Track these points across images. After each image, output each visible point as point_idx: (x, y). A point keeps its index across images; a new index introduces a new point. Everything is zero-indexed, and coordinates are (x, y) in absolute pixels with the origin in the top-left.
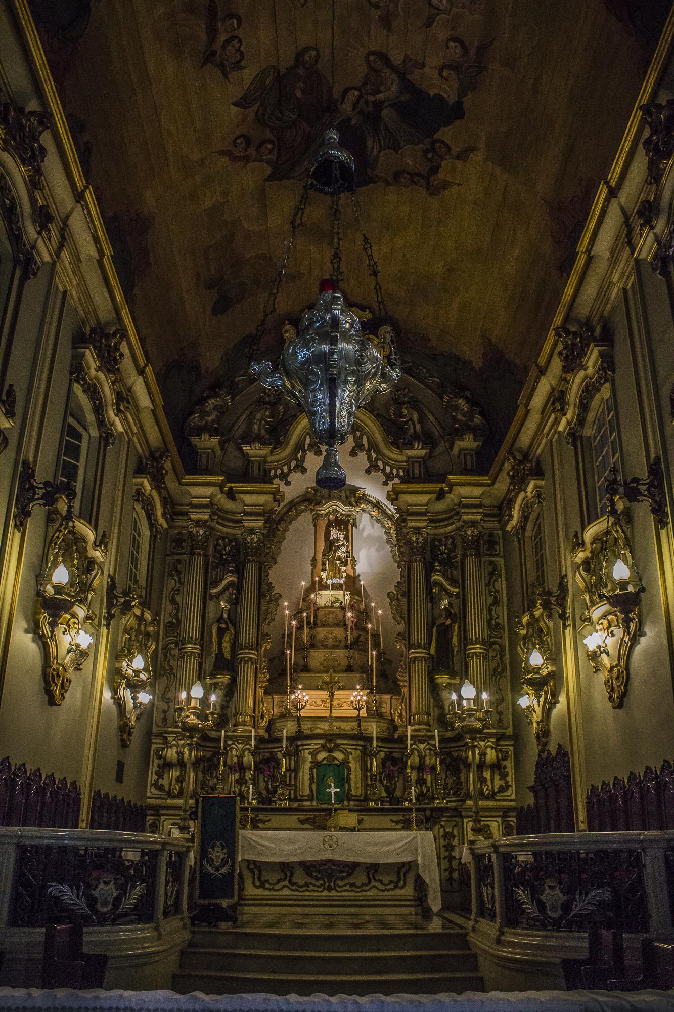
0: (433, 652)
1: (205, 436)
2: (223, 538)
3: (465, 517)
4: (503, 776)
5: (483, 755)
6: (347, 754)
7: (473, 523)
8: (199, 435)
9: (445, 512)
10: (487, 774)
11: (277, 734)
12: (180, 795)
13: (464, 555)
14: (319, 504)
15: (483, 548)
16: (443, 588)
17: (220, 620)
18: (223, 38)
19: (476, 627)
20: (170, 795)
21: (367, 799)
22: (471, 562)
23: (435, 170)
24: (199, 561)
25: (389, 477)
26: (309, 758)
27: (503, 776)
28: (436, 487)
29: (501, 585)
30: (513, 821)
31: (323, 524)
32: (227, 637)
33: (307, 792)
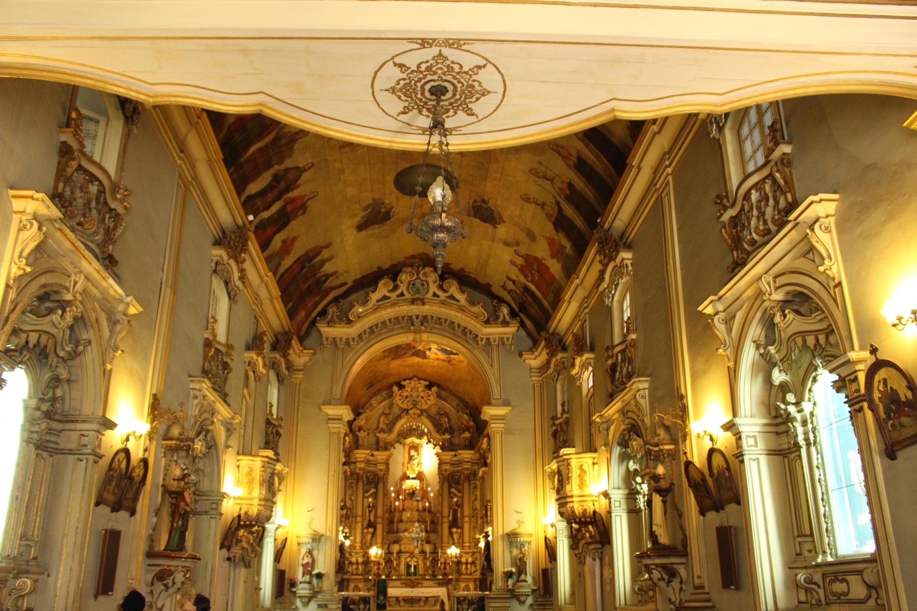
0: (451, 518)
1: (362, 432)
2: (369, 472)
3: (465, 466)
4: (475, 567)
5: (467, 560)
6: (418, 559)
7: (467, 469)
8: (359, 431)
9: (457, 461)
10: (469, 566)
11: (391, 551)
12: (357, 574)
13: (464, 482)
14: (405, 438)
15: (472, 477)
16: (455, 495)
17: (369, 506)
19: (467, 511)
20: (353, 574)
21: (425, 575)
22: (466, 484)
24: (360, 484)
25: (435, 446)
26: (404, 560)
27: (475, 567)
28: (453, 453)
29: (478, 492)
30: (478, 583)
31: (407, 448)
32: (372, 514)
33: (403, 573)
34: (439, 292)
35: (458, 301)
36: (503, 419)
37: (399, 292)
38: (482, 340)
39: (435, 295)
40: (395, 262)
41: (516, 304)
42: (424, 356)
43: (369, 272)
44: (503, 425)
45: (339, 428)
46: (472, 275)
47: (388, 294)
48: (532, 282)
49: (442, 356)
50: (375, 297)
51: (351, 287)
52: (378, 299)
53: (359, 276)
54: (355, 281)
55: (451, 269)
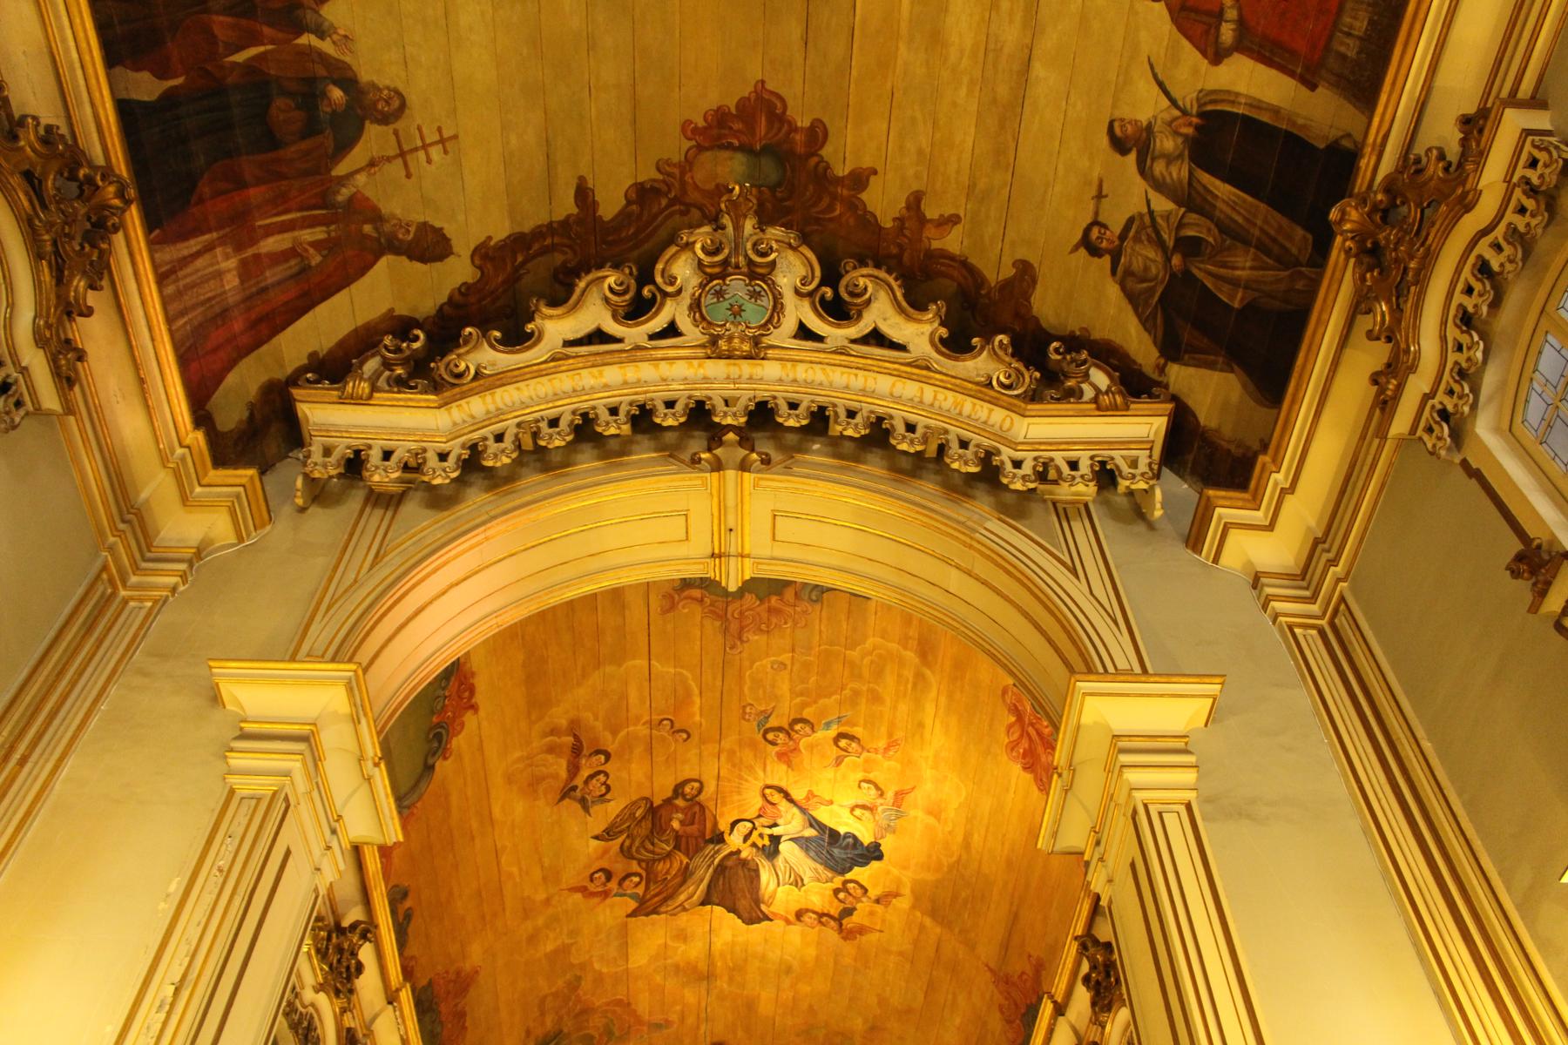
18: (585, 773)
23: (848, 912)
34: (816, 324)
35: (901, 347)
36: (1186, 752)
37: (658, 323)
38: (1017, 464)
39: (804, 333)
40: (648, 174)
41: (1146, 322)
42: (754, 913)
43: (542, 218)
44: (1190, 777)
45: (287, 774)
46: (953, 242)
47: (612, 328)
48: (1243, 45)
49: (818, 891)
50: (555, 327)
51: (466, 290)
52: (571, 337)
53: (500, 230)
54: (485, 254)
55: (867, 221)
